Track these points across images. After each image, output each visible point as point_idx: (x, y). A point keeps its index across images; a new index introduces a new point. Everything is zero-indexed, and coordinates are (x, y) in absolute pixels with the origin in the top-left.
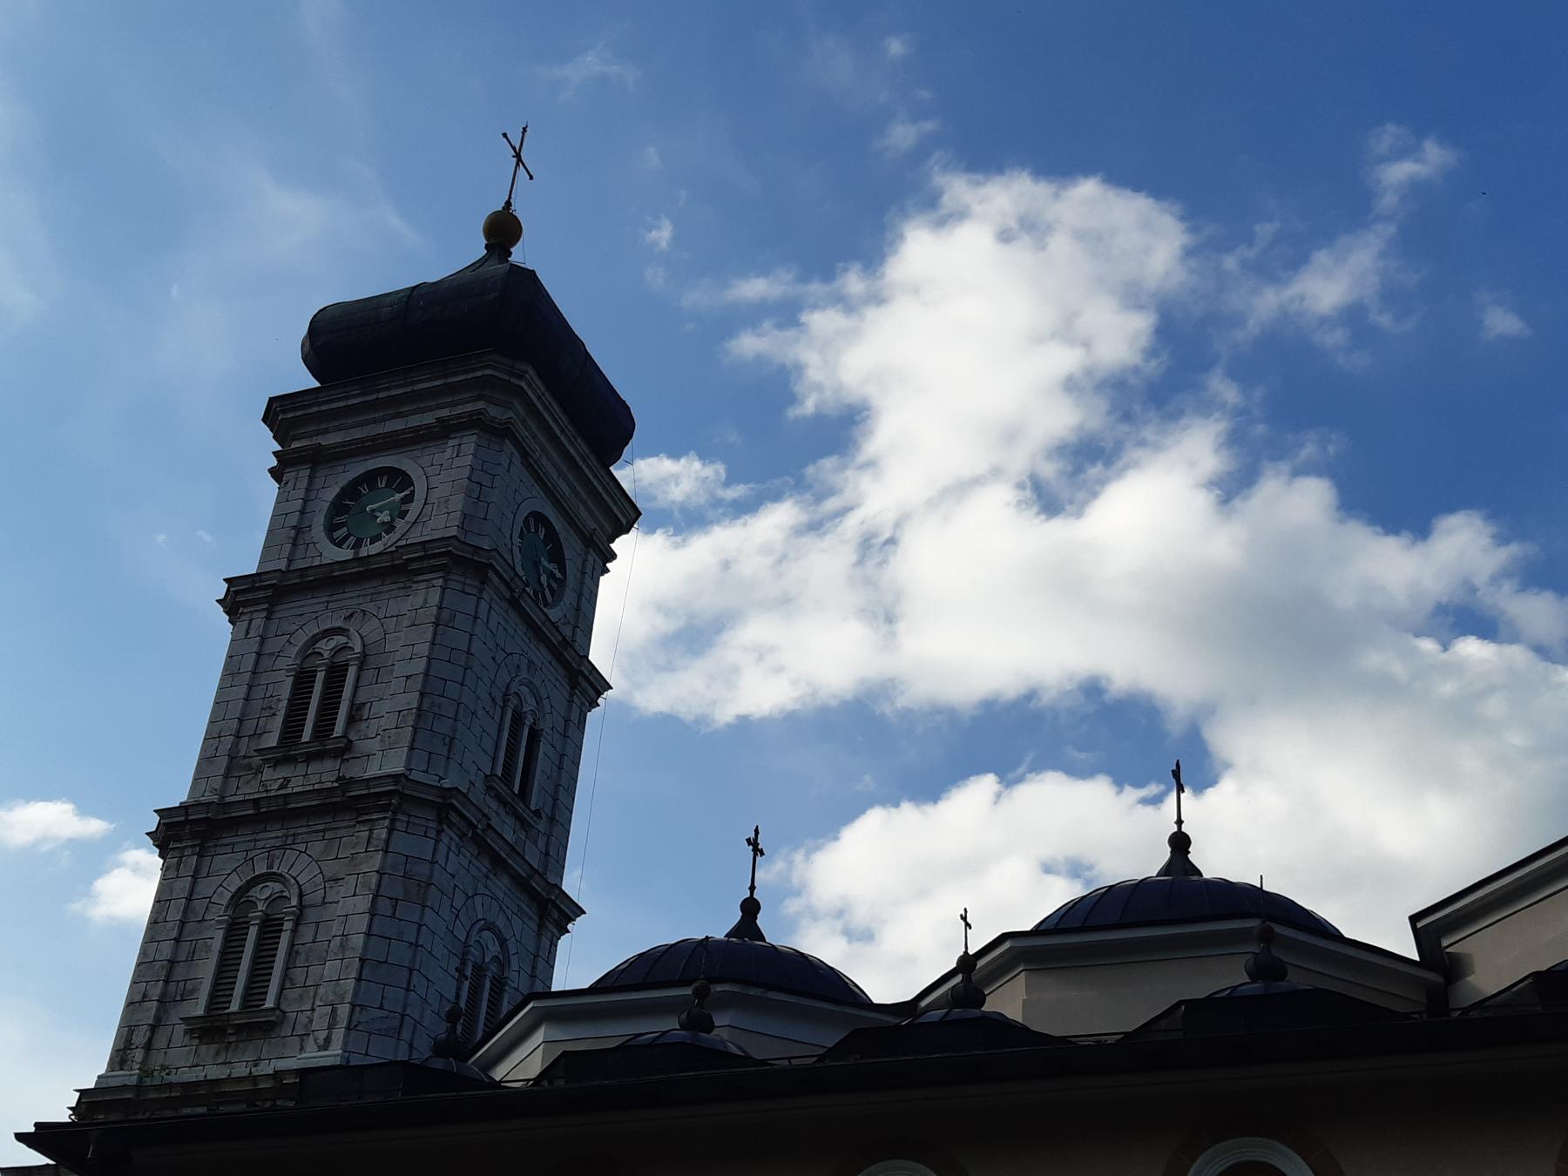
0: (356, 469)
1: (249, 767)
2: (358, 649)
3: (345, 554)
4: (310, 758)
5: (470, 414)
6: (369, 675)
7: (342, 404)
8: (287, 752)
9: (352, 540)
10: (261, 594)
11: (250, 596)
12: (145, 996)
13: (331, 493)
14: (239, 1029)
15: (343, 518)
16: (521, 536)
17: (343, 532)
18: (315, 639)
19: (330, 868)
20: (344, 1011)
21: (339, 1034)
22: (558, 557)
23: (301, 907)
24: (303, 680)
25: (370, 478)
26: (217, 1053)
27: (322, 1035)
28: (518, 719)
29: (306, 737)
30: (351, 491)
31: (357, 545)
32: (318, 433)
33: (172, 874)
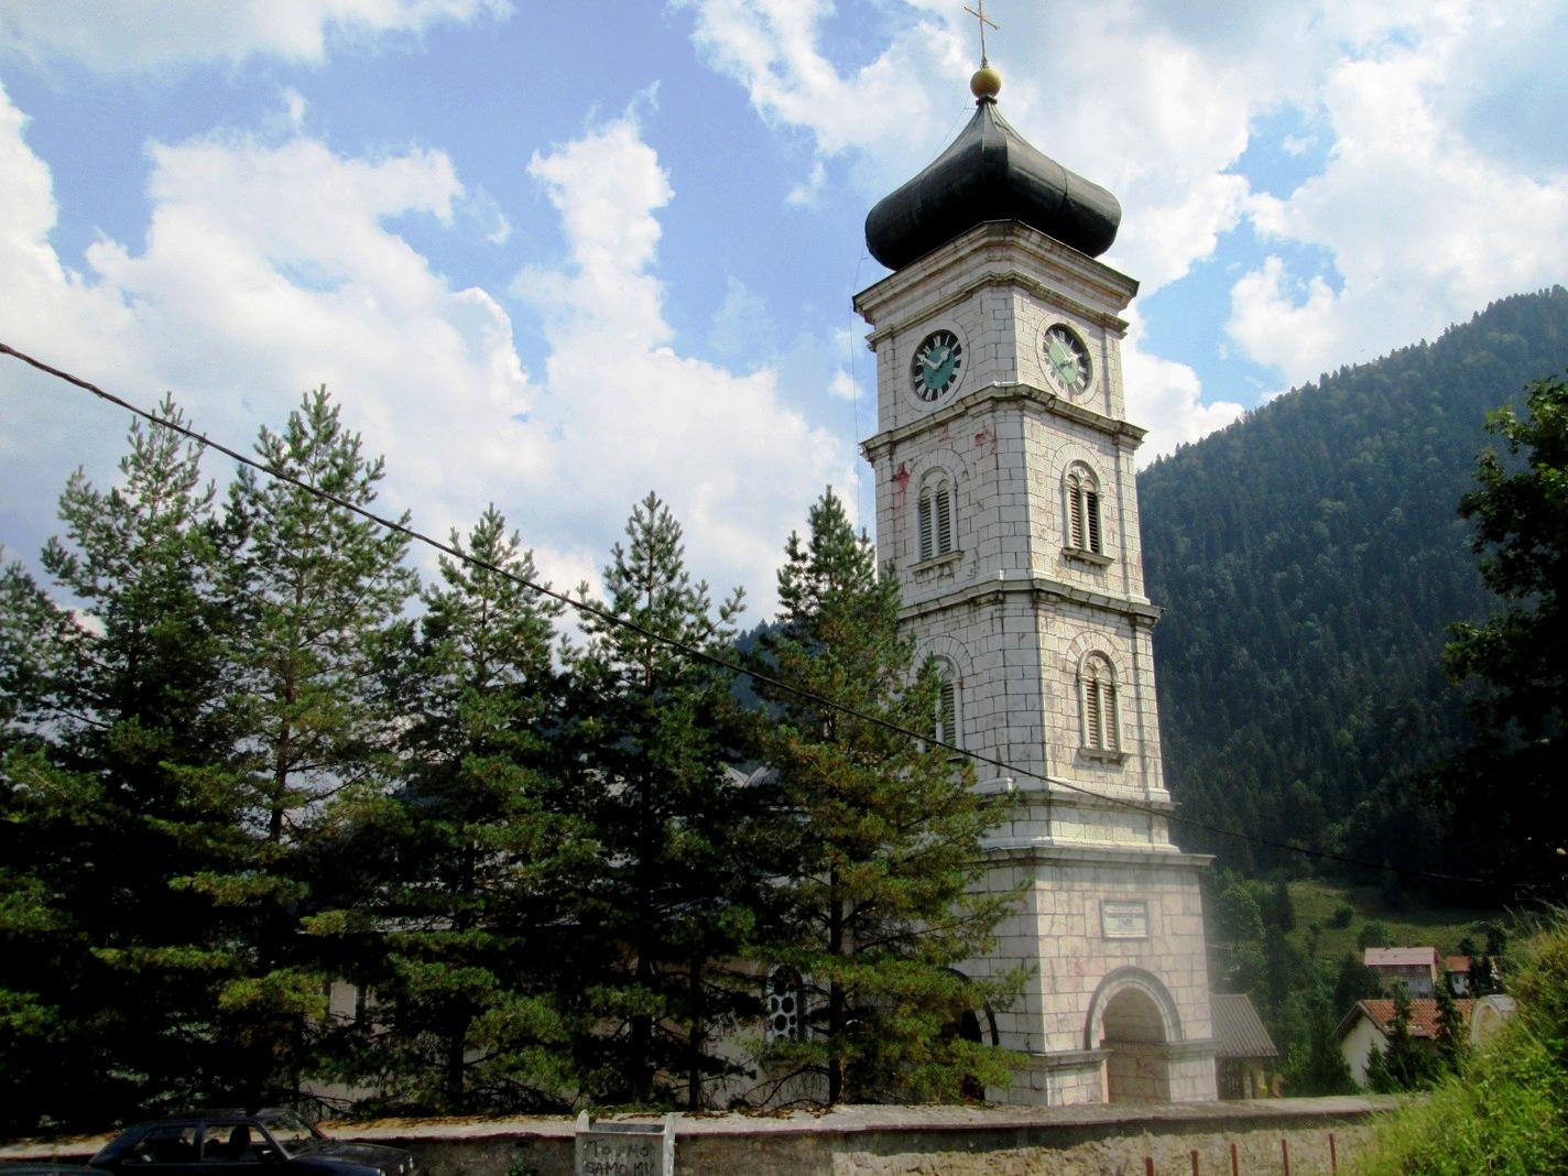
0: (919, 335)
2: (952, 482)
6: (962, 501)
9: (930, 392)
13: (907, 362)
15: (920, 377)
16: (1046, 350)
17: (922, 388)
18: (924, 478)
22: (1078, 346)
23: (962, 678)
24: (924, 507)
25: (929, 341)
28: (1077, 495)
29: (935, 553)
31: (935, 397)
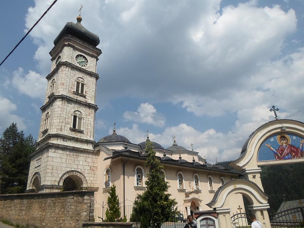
1: (71, 92)
3: (80, 66)
4: (80, 96)
5: (96, 56)
7: (79, 42)
8: (76, 93)
10: (70, 66)
11: (68, 65)
12: (63, 122)
14: (78, 131)
18: (79, 78)
19: (87, 113)
20: (92, 133)
21: (92, 136)
24: (78, 83)
25: (81, 55)
26: (75, 134)
27: (90, 136)
29: (80, 92)
30: (78, 56)
32: (74, 43)
33: (63, 104)
